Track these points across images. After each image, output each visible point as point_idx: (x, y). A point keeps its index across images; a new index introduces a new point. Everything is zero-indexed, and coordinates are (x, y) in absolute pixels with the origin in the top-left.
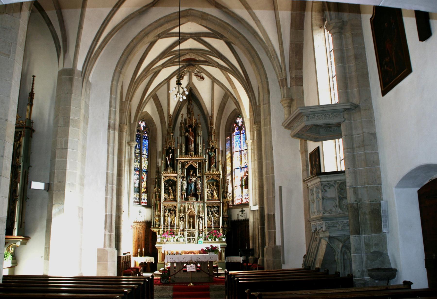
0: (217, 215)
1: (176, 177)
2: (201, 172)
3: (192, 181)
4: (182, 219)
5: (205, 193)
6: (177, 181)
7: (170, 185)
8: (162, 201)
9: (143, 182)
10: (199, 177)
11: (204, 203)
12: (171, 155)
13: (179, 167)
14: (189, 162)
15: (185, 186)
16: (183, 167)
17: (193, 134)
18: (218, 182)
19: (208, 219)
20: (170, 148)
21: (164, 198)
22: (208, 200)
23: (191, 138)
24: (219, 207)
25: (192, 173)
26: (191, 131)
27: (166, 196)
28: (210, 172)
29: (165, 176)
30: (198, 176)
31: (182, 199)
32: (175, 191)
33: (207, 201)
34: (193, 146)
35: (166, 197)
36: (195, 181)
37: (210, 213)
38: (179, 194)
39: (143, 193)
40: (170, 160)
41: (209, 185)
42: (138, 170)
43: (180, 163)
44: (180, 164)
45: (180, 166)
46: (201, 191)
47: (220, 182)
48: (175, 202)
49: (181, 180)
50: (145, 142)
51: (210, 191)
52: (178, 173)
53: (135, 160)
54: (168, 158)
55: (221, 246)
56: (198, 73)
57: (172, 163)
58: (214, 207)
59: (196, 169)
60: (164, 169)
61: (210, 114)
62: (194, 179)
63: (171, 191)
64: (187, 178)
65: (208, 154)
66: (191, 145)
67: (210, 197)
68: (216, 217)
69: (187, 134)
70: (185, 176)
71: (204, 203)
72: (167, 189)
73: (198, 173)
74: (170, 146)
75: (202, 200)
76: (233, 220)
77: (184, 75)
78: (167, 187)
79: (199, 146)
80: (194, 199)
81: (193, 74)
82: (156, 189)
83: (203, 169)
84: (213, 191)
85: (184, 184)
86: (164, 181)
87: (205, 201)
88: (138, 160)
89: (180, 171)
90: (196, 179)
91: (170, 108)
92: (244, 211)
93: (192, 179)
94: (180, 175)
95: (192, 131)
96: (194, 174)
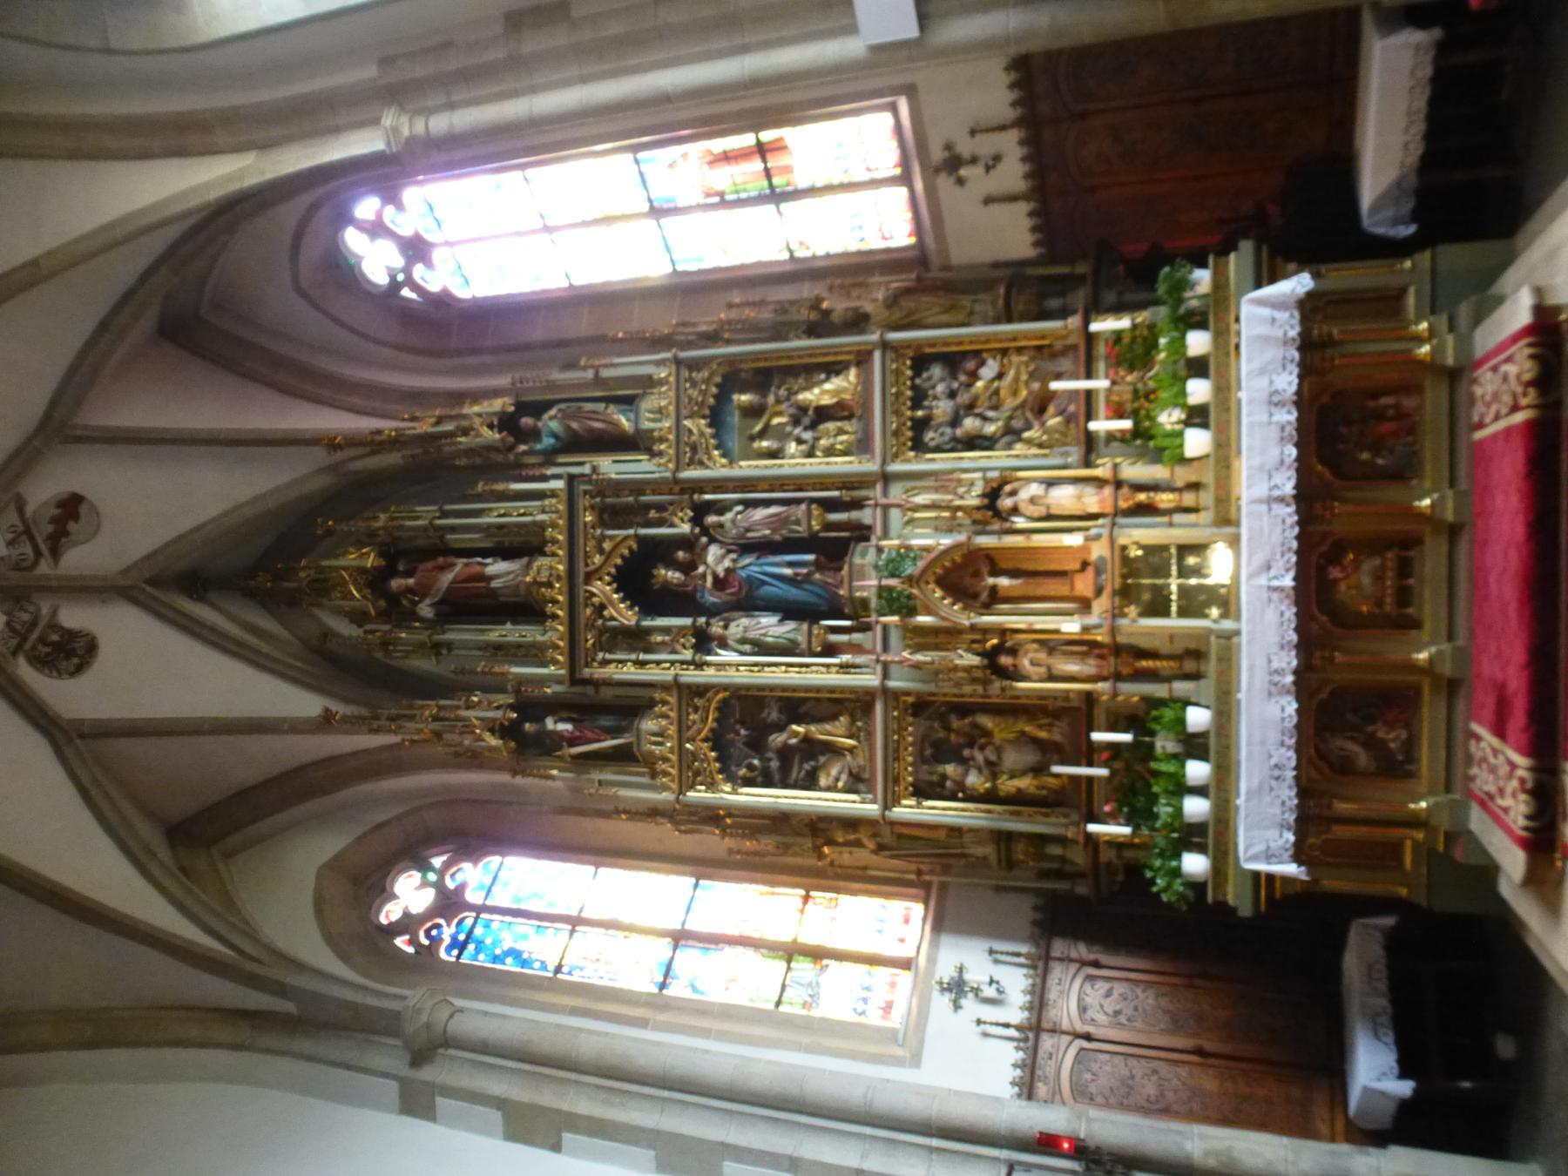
0: (989, 370)
1: (701, 690)
2: (661, 507)
3: (728, 571)
4: (1005, 660)
5: (817, 465)
6: (725, 688)
7: (757, 745)
8: (872, 809)
10: (697, 521)
11: (887, 478)
12: (550, 724)
13: (629, 673)
14: (593, 595)
15: (769, 626)
16: (636, 639)
17: (430, 565)
18: (733, 378)
19: (1020, 440)
20: (505, 731)
21: (848, 790)
22: (862, 446)
23: (447, 578)
24: (921, 362)
25: (674, 576)
26: (411, 581)
27: (834, 771)
28: (662, 440)
30: (685, 528)
31: (857, 649)
32: (798, 705)
33: (873, 457)
34: (496, 567)
35: (844, 777)
36: (730, 551)
37: (970, 424)
38: (819, 674)
40: (589, 735)
41: (756, 445)
43: (605, 663)
44: (610, 662)
45: (620, 662)
46: (798, 501)
47: (731, 360)
48: (879, 708)
49: (726, 656)
51: (797, 431)
52: (667, 675)
54: (573, 742)
55: (1258, 284)
56: (32, 538)
57: (606, 721)
58: (919, 399)
59: (642, 540)
60: (645, 780)
61: (319, 456)
62: (710, 559)
63: (796, 734)
64: (712, 612)
65: (549, 457)
66: (495, 584)
67: (841, 432)
68: (1000, 376)
69: (426, 610)
70: (687, 621)
71: (887, 478)
72: (785, 768)
73: (672, 525)
74: (492, 731)
75: (863, 493)
76: (1036, 244)
77: (54, 626)
78: (775, 764)
79: (501, 527)
80: (863, 555)
81: (44, 567)
83: (638, 487)
84: (803, 409)
85: (752, 635)
86: (727, 787)
87: (871, 466)
89: (658, 663)
90: (713, 540)
91: (284, 720)
92: (948, 147)
93: (715, 577)
94: (682, 663)
95: (409, 573)
96: (681, 554)
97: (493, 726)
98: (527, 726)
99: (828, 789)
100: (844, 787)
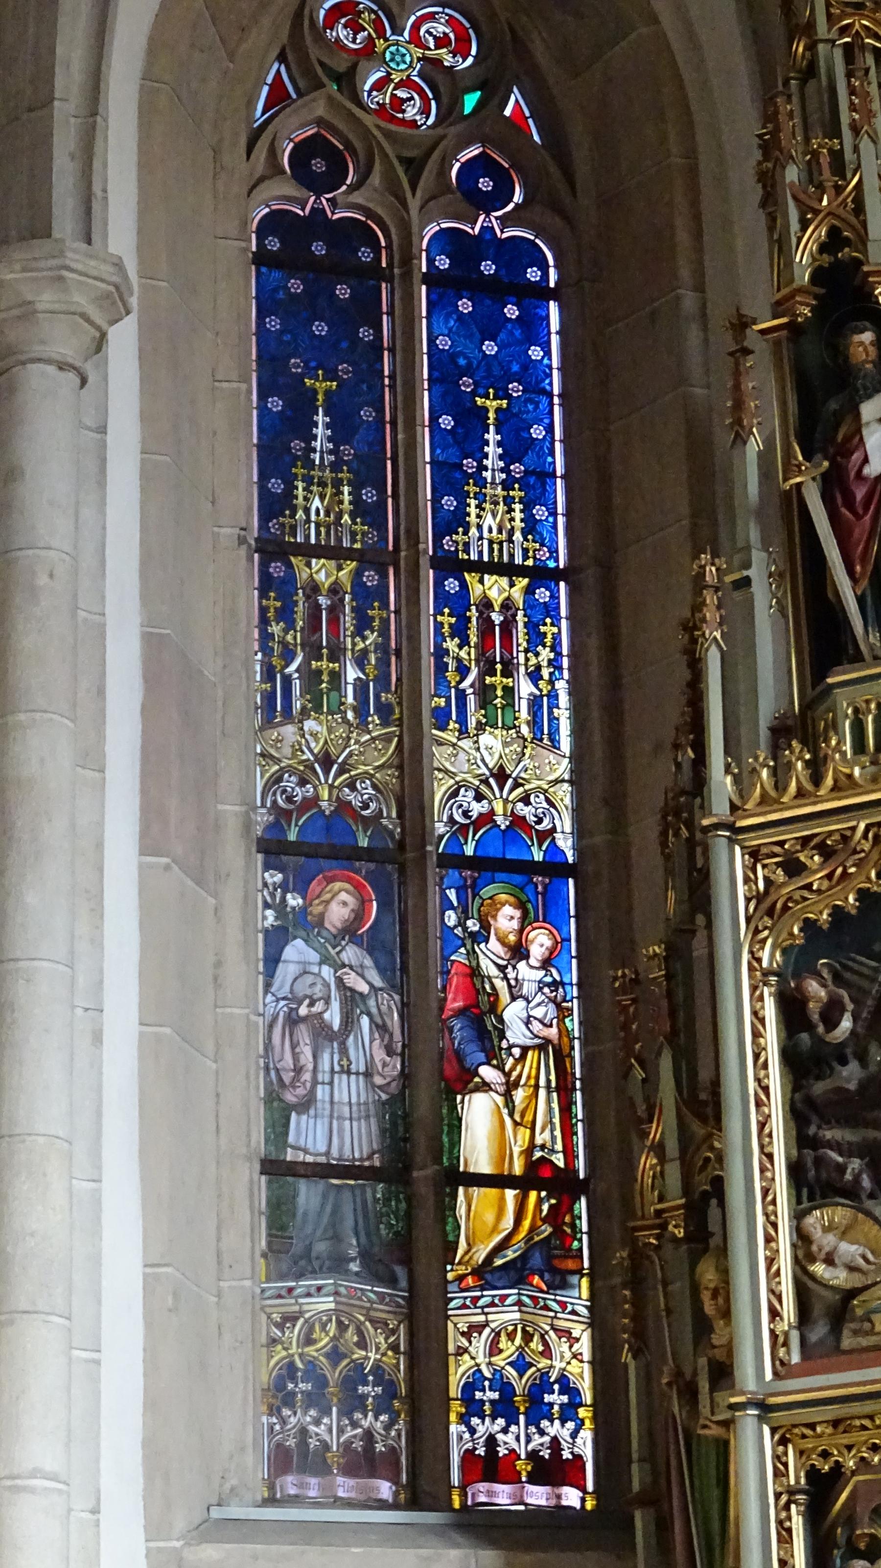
9: (487, 1073)
29: (790, 835)
35: (838, 1277)
39: (479, 1272)
42: (354, 854)
50: (490, 348)
53: (269, 674)
82: (659, 1149)
88: (352, 673)
97: (847, 242)
98: (867, 337)
99: (802, 1238)
100: (812, 1277)
